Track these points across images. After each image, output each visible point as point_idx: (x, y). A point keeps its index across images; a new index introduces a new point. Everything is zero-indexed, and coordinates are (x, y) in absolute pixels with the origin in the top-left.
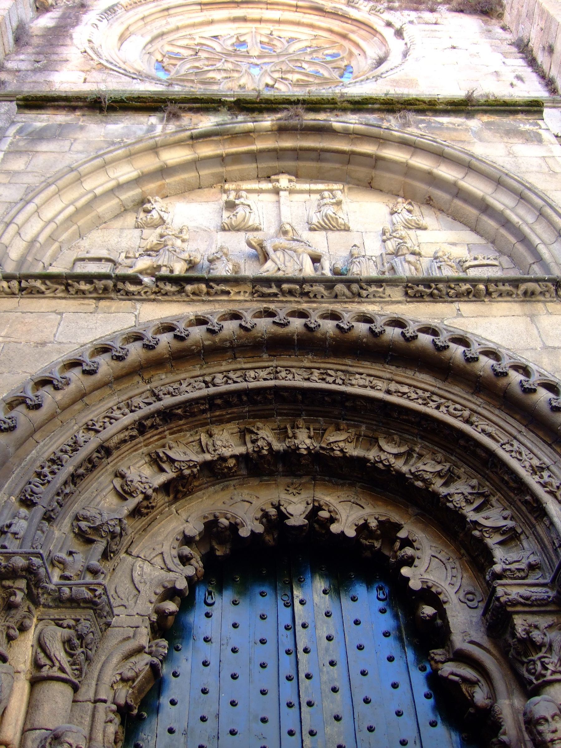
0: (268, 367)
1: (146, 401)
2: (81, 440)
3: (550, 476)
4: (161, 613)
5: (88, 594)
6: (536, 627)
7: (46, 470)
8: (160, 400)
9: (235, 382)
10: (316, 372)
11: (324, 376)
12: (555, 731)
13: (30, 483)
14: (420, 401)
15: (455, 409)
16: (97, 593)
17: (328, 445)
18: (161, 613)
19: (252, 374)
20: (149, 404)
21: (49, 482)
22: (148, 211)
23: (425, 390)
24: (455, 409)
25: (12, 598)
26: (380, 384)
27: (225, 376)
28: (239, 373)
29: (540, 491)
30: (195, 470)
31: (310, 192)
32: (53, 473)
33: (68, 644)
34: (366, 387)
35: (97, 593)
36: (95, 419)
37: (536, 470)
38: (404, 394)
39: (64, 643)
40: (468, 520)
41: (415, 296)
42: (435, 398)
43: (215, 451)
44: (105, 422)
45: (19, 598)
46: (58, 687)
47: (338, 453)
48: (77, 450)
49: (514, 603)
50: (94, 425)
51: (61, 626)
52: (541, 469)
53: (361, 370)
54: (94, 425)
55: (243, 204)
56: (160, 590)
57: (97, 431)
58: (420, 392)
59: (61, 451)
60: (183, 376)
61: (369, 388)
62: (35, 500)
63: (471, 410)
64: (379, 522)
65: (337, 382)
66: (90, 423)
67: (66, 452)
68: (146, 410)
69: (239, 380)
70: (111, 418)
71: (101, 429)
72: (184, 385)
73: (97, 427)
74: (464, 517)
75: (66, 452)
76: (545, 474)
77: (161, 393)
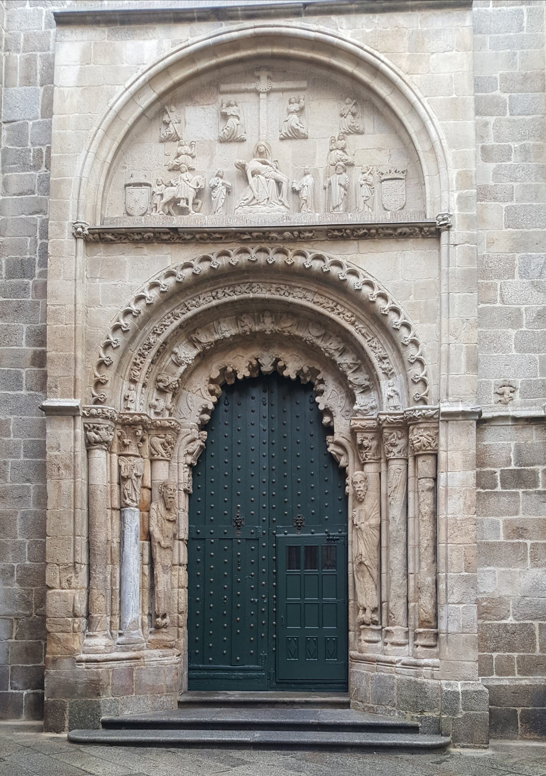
0: (247, 283)
1: (182, 311)
2: (152, 341)
3: (388, 363)
4: (202, 420)
5: (168, 424)
6: (367, 438)
7: (138, 361)
8: (189, 310)
9: (229, 295)
10: (274, 286)
11: (279, 289)
12: (360, 487)
13: (132, 370)
14: (330, 310)
15: (347, 316)
16: (172, 424)
17: (282, 329)
18: (202, 420)
19: (238, 289)
20: (183, 314)
21: (141, 368)
22: (167, 124)
23: (334, 301)
24: (347, 316)
25: (137, 434)
26: (309, 296)
27: (223, 292)
28: (231, 289)
29: (380, 372)
30: (212, 346)
31: (283, 90)
32: (141, 362)
33: (162, 444)
34: (301, 298)
35: (172, 424)
36: (157, 326)
37: (382, 359)
38: (321, 304)
39: (161, 445)
40: (348, 378)
41: (332, 237)
42: (338, 307)
43: (222, 333)
44: (162, 329)
45: (140, 433)
46: (162, 463)
47: (287, 333)
48: (151, 348)
49: (359, 428)
50: (157, 330)
51: (159, 437)
52: (385, 358)
53: (299, 285)
54: (157, 330)
55: (232, 115)
56: (201, 410)
57: (159, 335)
58: (330, 302)
59: (144, 349)
60: (201, 292)
61: (303, 299)
62: (137, 380)
63: (356, 316)
64: (309, 368)
65: (286, 294)
66: (155, 329)
67: (146, 349)
68: (183, 318)
69: (232, 294)
70: (165, 326)
71: (160, 332)
72: (201, 300)
73: (159, 332)
74: (346, 377)
75: (146, 349)
76: (385, 361)
77: (189, 306)
